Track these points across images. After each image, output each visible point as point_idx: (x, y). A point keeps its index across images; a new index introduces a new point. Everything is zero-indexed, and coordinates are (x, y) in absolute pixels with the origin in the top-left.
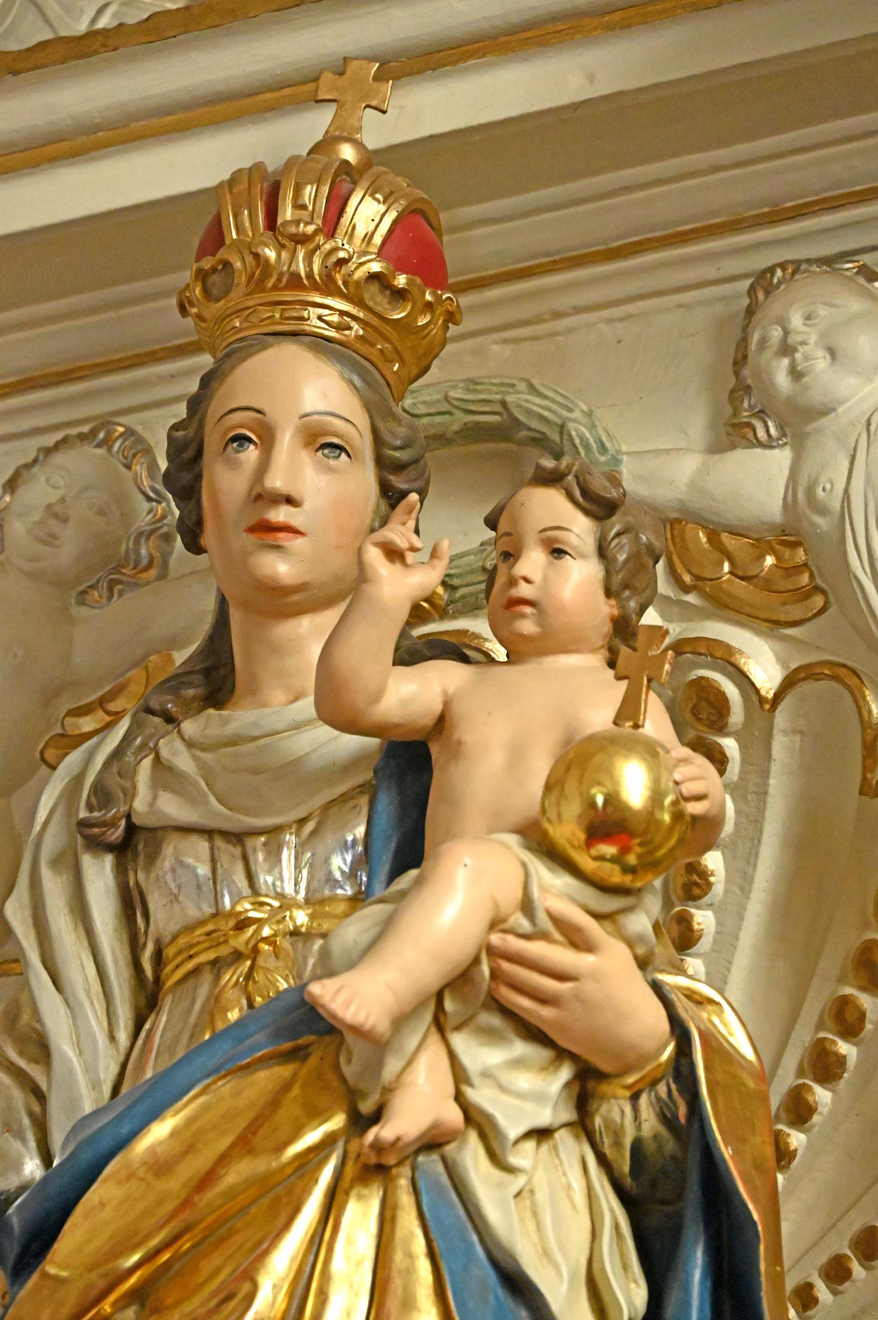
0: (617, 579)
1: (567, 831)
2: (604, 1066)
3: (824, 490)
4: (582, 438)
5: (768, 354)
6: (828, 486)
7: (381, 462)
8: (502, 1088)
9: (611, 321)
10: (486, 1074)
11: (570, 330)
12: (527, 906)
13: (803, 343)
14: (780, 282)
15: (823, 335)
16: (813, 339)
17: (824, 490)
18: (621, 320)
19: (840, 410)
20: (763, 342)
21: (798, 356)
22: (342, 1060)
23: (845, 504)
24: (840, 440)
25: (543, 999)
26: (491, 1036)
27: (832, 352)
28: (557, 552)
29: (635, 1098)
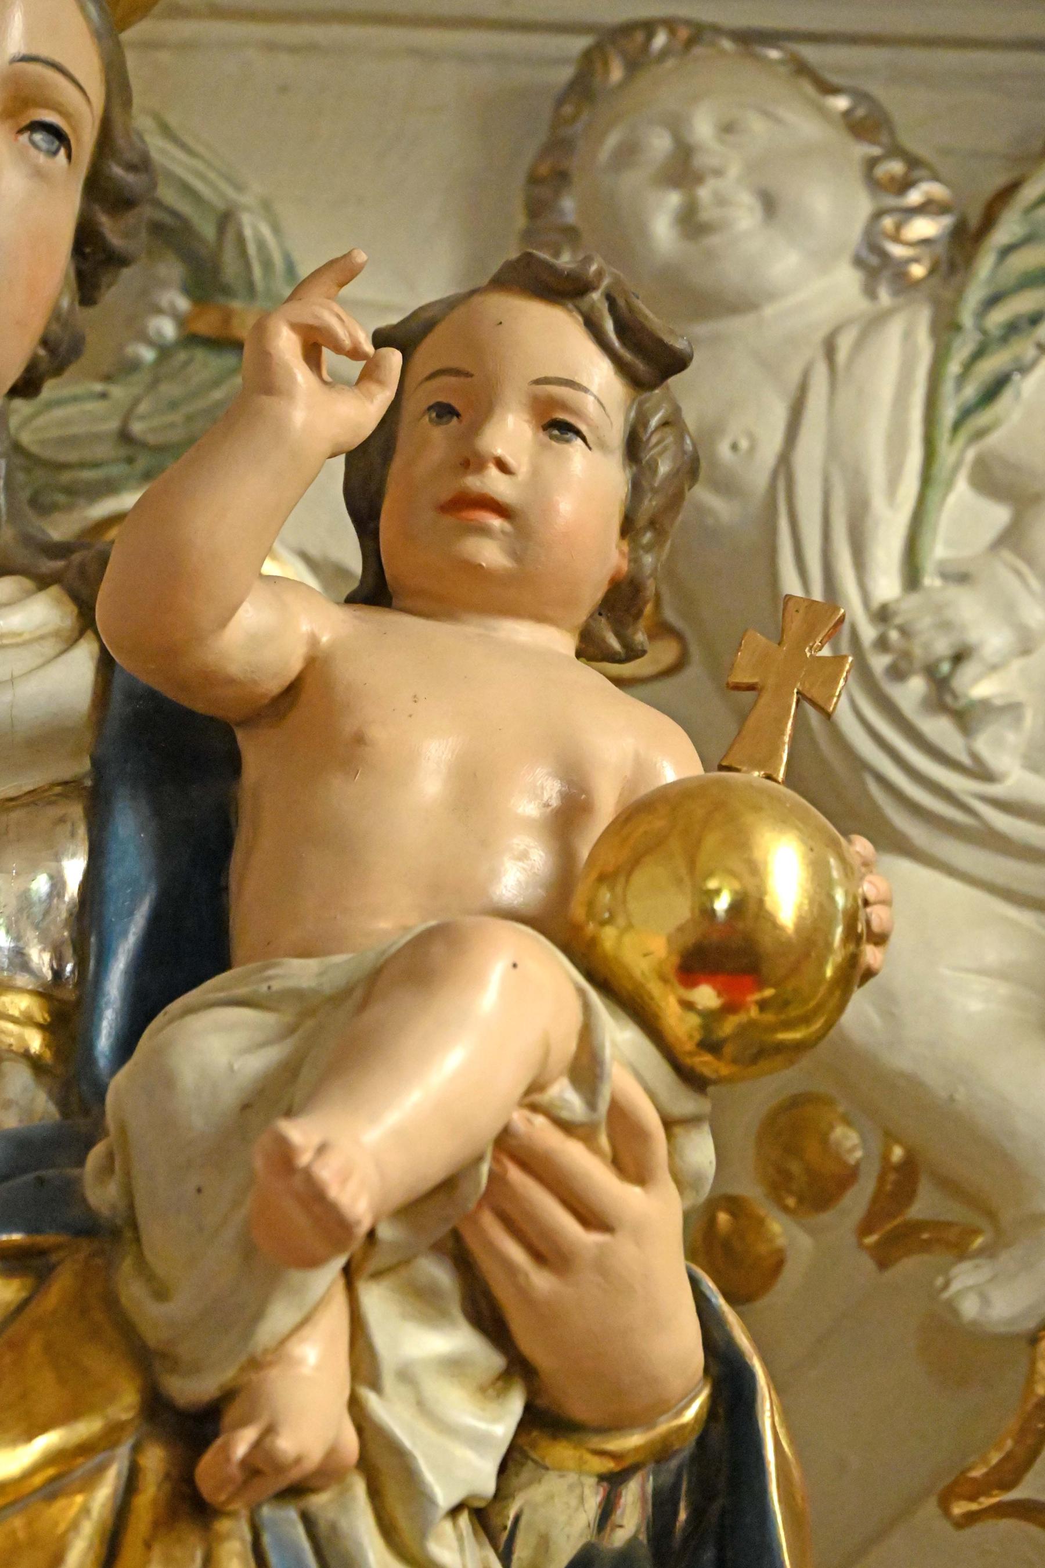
0: (650, 504)
1: (644, 946)
2: (578, 1409)
3: (734, 447)
4: (261, 245)
5: (632, 180)
6: (744, 444)
7: (99, 190)
8: (421, 1406)
9: (271, 47)
10: (406, 1376)
11: (186, 47)
12: (586, 1070)
13: (718, 173)
14: (665, 53)
15: (753, 167)
16: (734, 170)
17: (734, 447)
18: (293, 49)
19: (769, 311)
20: (628, 153)
21: (704, 193)
22: (133, 1292)
23: (781, 485)
24: (769, 365)
25: (547, 1253)
26: (424, 1302)
27: (769, 204)
28: (558, 427)
29: (613, 1482)
